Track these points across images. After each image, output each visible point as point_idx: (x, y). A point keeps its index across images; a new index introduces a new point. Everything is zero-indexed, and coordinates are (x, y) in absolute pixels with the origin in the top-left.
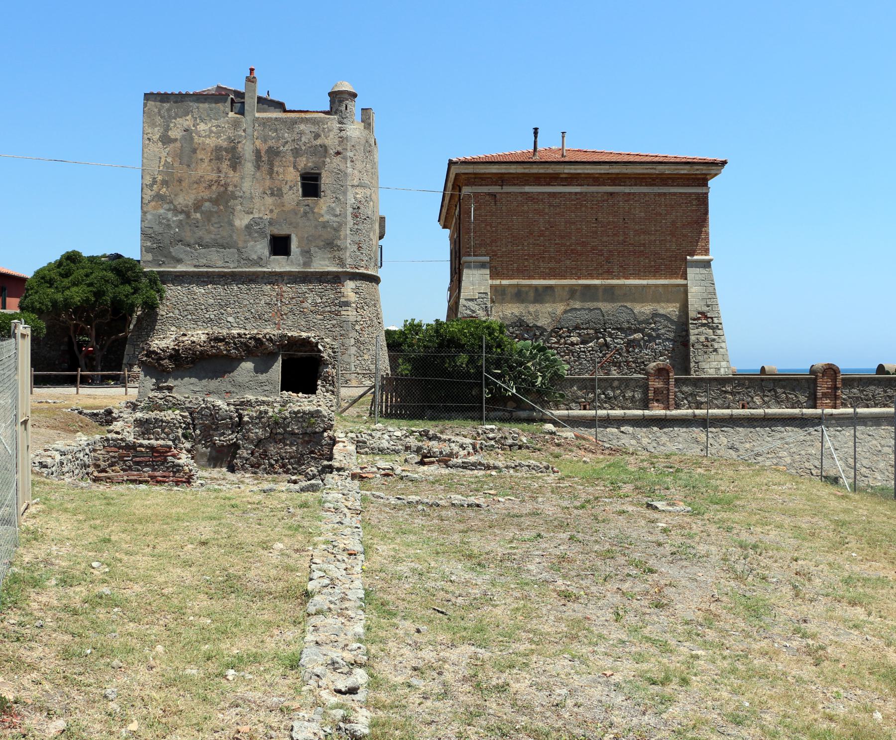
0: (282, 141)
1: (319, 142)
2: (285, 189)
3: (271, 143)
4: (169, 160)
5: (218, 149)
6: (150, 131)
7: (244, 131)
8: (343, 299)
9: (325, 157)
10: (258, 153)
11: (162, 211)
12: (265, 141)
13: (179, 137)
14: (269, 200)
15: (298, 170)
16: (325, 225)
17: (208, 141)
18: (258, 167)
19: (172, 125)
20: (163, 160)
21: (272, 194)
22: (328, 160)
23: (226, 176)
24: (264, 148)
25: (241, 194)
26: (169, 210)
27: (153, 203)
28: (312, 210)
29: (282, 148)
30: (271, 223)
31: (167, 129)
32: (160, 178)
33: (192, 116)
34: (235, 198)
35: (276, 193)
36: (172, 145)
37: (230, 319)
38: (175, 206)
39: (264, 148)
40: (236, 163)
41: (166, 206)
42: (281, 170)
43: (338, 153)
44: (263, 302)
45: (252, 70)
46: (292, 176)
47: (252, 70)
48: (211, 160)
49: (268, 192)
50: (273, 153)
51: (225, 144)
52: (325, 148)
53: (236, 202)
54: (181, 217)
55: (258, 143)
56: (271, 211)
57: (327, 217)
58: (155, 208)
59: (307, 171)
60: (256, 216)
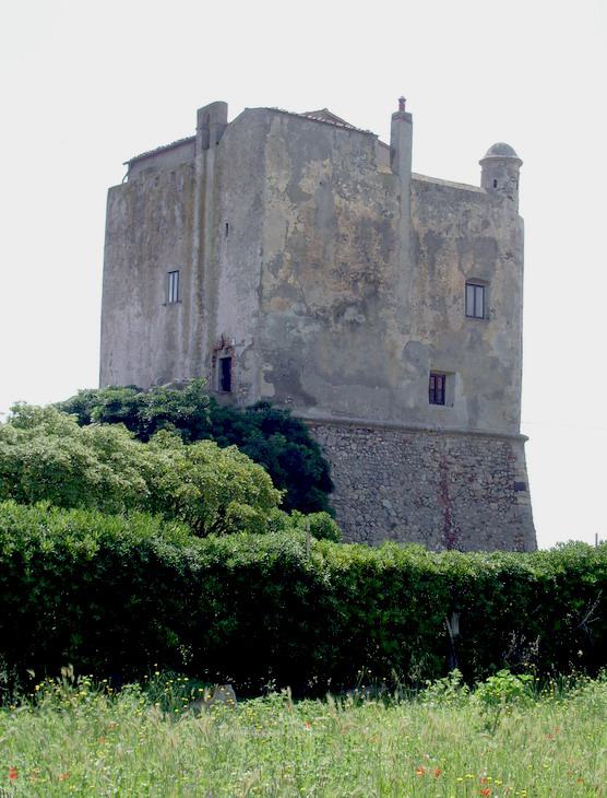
0: (445, 224)
1: (487, 234)
2: (449, 301)
3: (432, 225)
4: (300, 227)
5: (364, 223)
6: (273, 174)
7: (399, 198)
8: (518, 480)
9: (496, 258)
10: (415, 236)
11: (290, 314)
12: (424, 221)
13: (312, 192)
14: (430, 315)
15: (463, 271)
16: (495, 362)
17: (352, 206)
18: (417, 262)
19: (304, 171)
20: (291, 229)
21: (433, 307)
22: (498, 261)
23: (376, 269)
24: (423, 231)
25: (396, 301)
26: (300, 313)
27: (278, 299)
28: (480, 336)
29: (444, 235)
30: (435, 354)
31: (297, 177)
32: (288, 256)
33: (331, 161)
34: (388, 306)
35: (439, 303)
36: (304, 204)
37: (386, 503)
38: (308, 310)
39: (423, 231)
40: (389, 250)
41: (295, 306)
42: (444, 268)
43: (510, 255)
44: (424, 477)
45: (402, 101)
46: (455, 279)
47: (402, 101)
48: (357, 238)
49: (429, 301)
50: (434, 242)
51: (374, 216)
52: (494, 242)
53: (389, 312)
54: (316, 327)
55: (416, 221)
56: (433, 332)
57: (496, 353)
58: (282, 307)
59: (475, 276)
60: (414, 339)
